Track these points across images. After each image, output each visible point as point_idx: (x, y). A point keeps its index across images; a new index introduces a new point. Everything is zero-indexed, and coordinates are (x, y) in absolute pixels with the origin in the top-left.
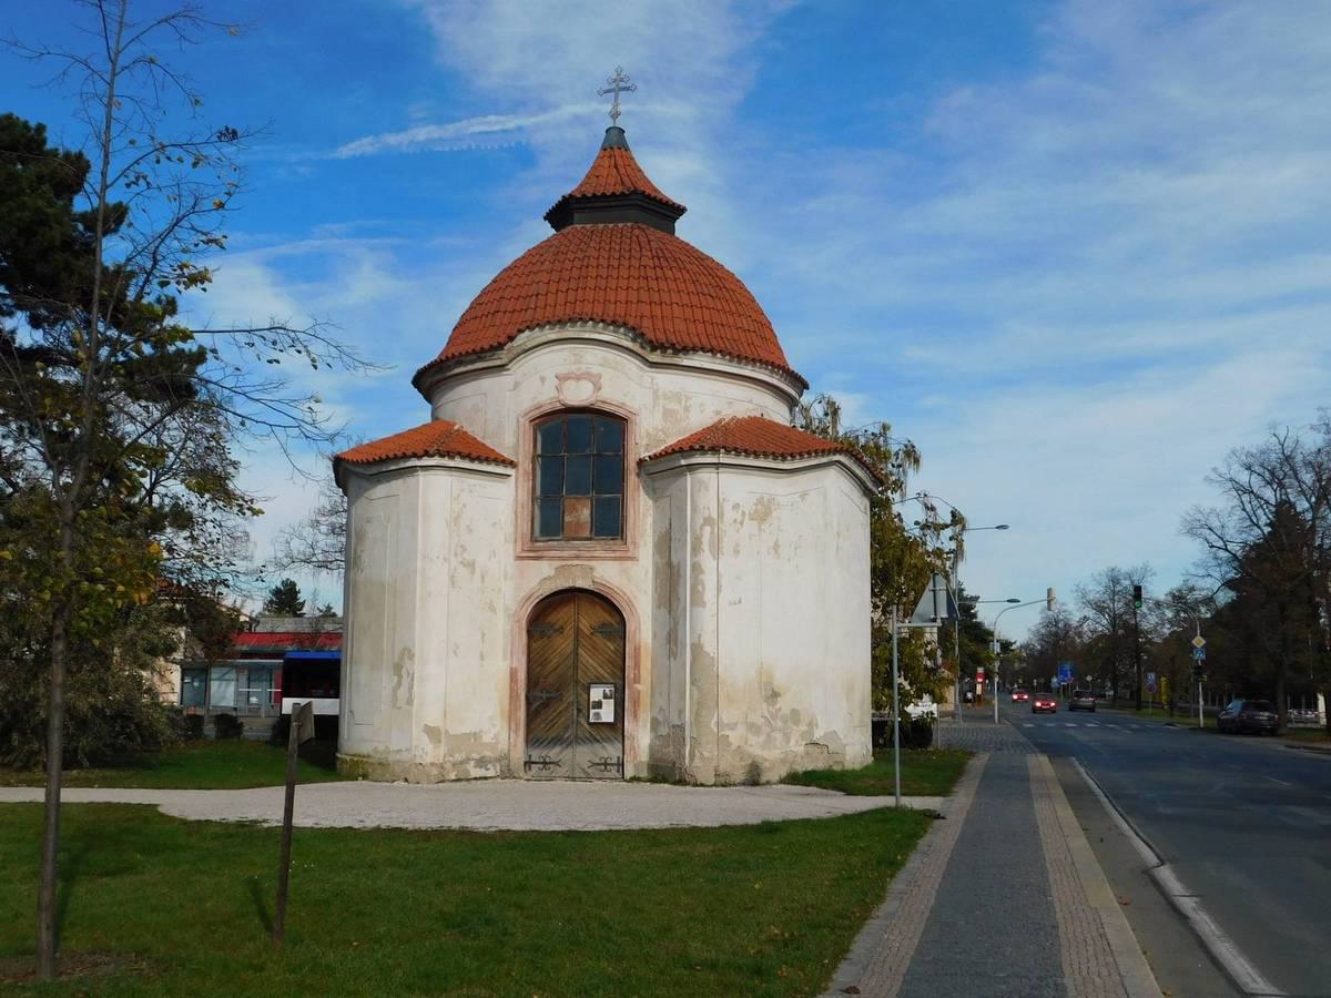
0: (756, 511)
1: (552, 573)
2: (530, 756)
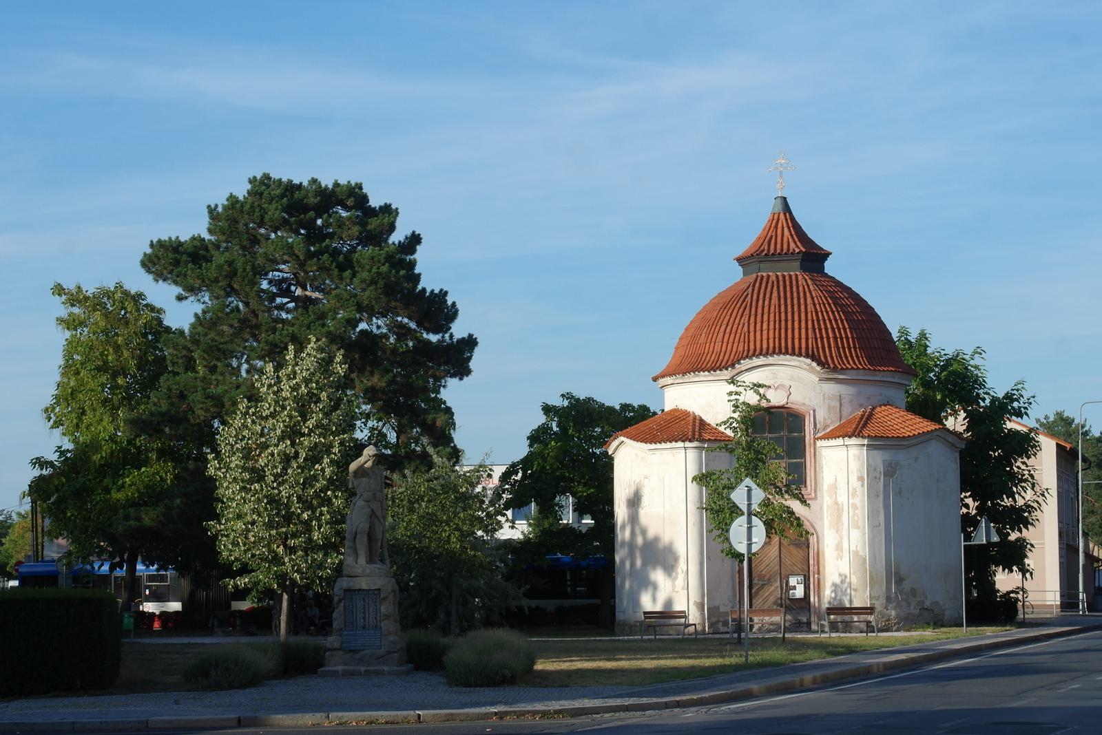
0: (888, 470)
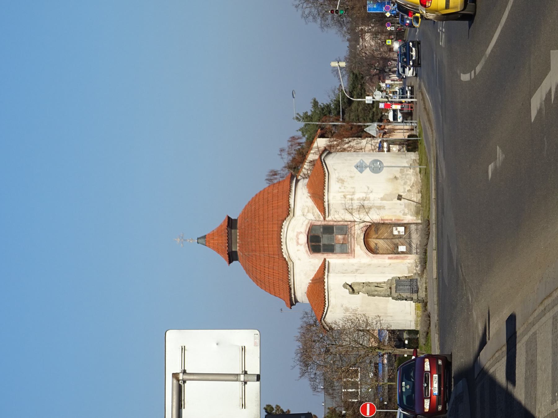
1: (359, 246)
2: (415, 253)
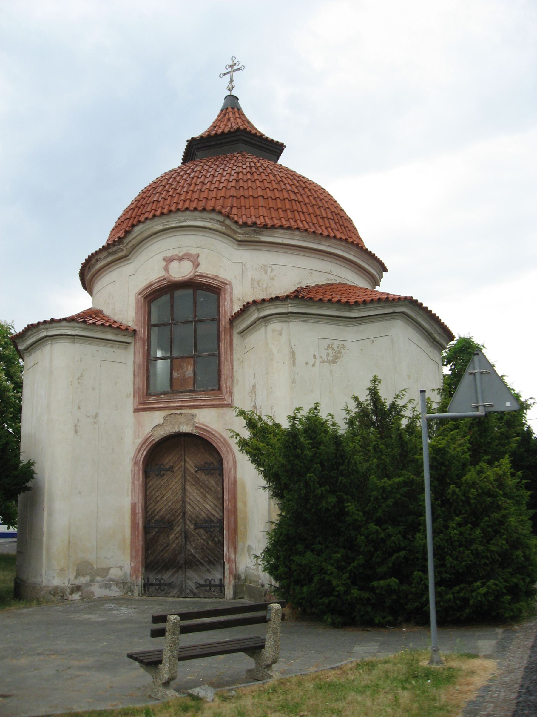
1: (162, 421)
2: (148, 579)
